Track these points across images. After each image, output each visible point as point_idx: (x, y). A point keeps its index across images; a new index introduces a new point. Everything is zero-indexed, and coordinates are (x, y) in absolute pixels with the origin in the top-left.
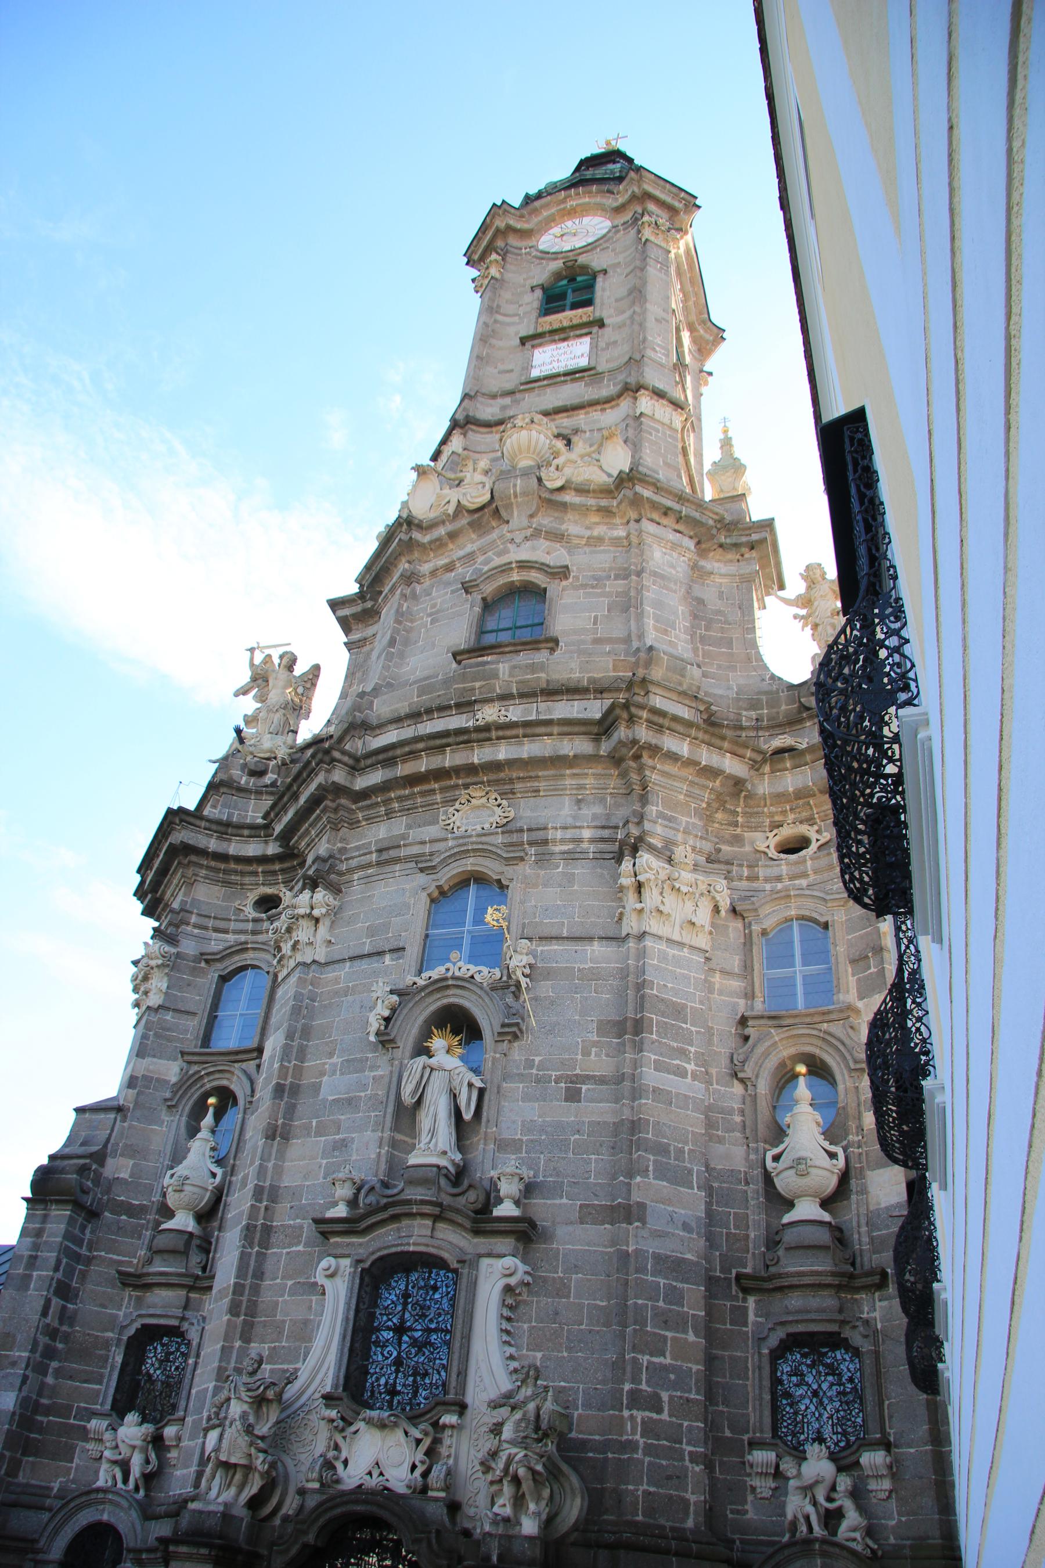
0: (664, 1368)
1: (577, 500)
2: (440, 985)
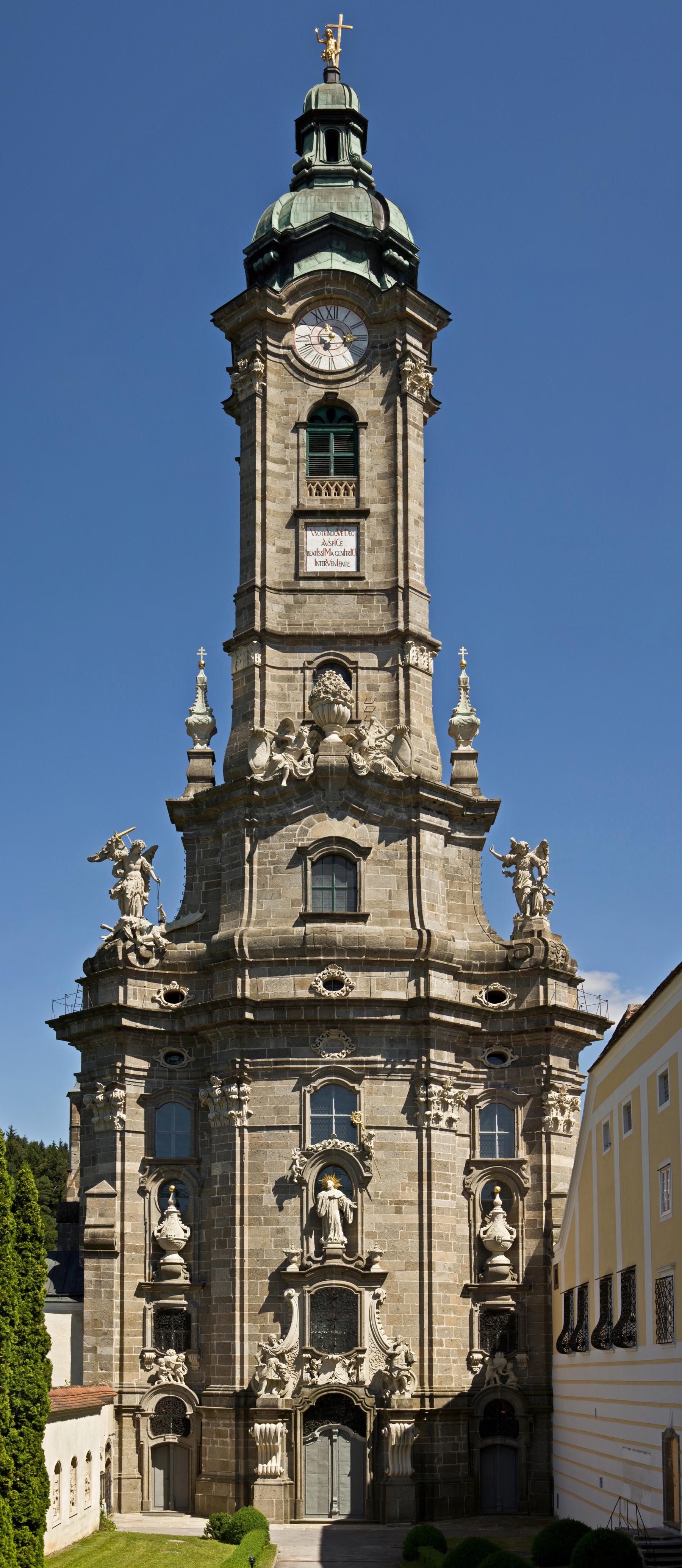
0: (443, 1329)
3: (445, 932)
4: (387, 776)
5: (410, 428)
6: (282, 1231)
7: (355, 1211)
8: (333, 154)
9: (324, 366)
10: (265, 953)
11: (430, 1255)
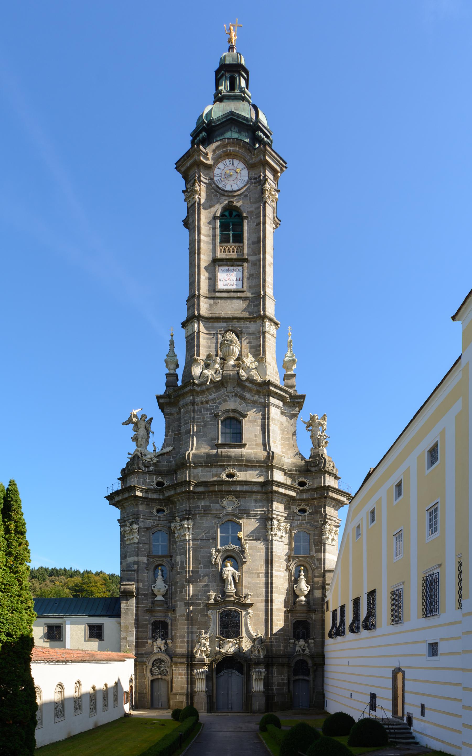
1: (250, 385)
2: (227, 551)
3: (280, 453)
4: (255, 380)
5: (267, 219)
7: (239, 576)
8: (232, 88)
11: (272, 596)
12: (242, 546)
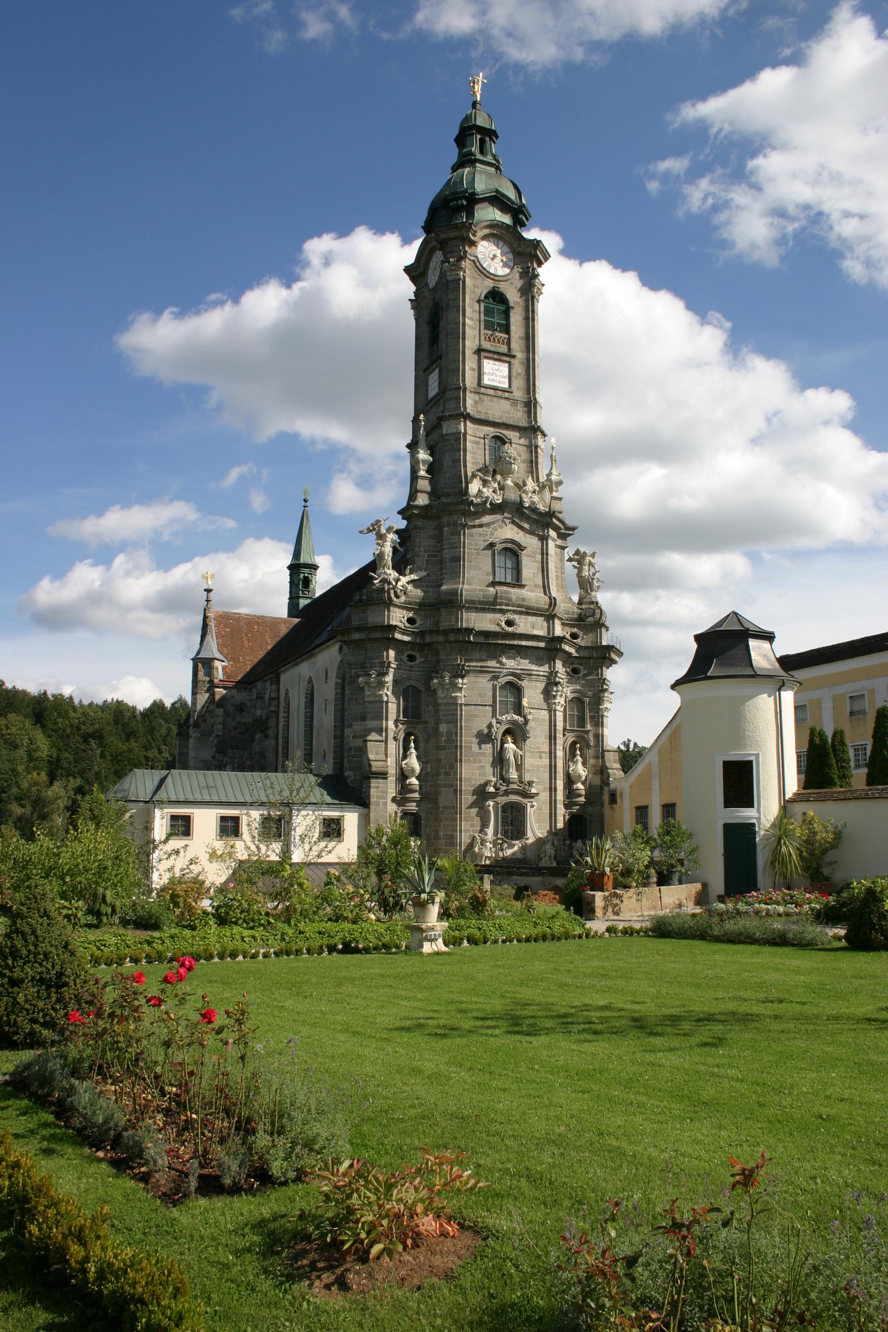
6: (483, 767)
9: (492, 271)
10: (473, 602)
12: (525, 717)
